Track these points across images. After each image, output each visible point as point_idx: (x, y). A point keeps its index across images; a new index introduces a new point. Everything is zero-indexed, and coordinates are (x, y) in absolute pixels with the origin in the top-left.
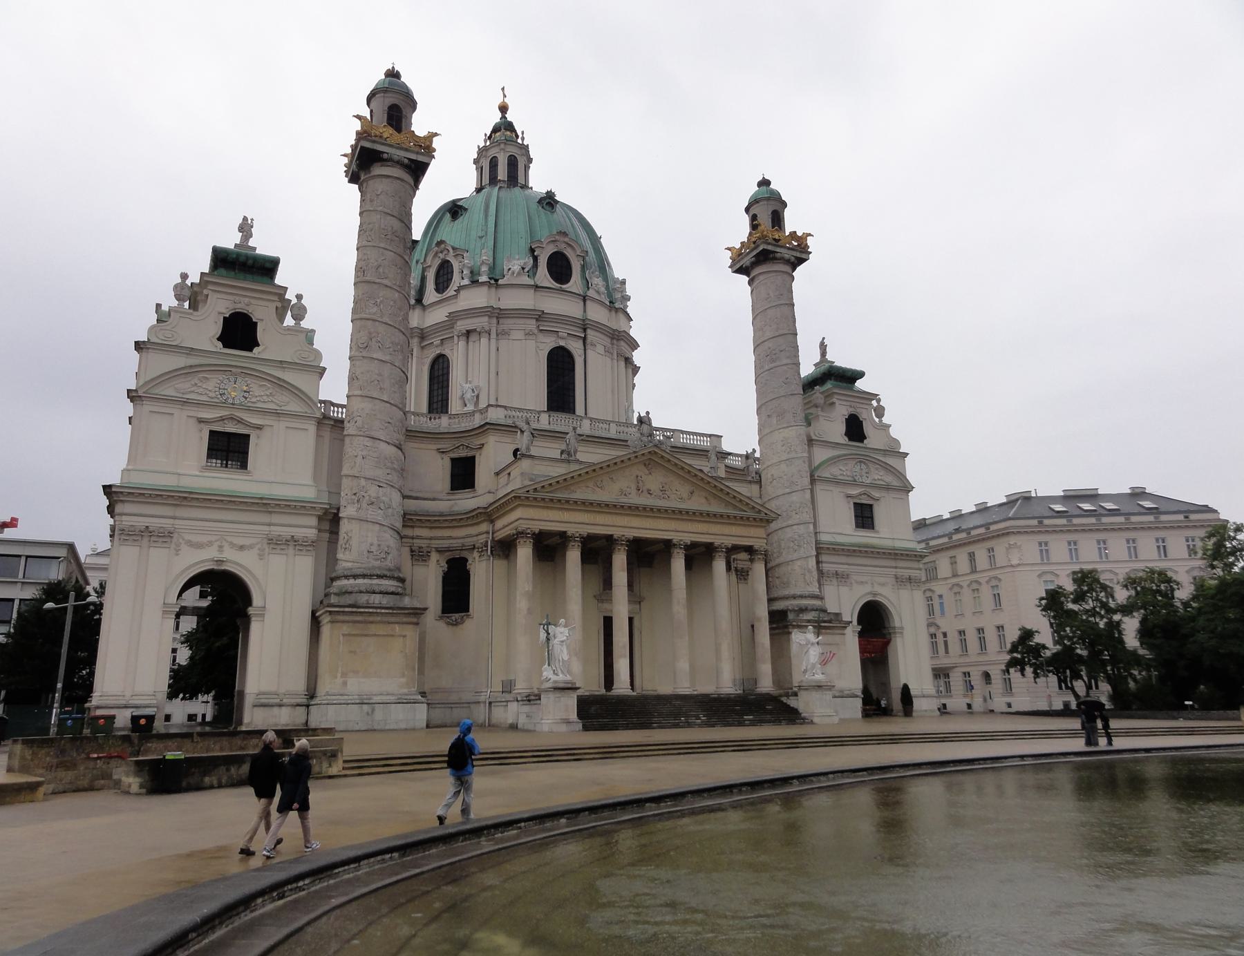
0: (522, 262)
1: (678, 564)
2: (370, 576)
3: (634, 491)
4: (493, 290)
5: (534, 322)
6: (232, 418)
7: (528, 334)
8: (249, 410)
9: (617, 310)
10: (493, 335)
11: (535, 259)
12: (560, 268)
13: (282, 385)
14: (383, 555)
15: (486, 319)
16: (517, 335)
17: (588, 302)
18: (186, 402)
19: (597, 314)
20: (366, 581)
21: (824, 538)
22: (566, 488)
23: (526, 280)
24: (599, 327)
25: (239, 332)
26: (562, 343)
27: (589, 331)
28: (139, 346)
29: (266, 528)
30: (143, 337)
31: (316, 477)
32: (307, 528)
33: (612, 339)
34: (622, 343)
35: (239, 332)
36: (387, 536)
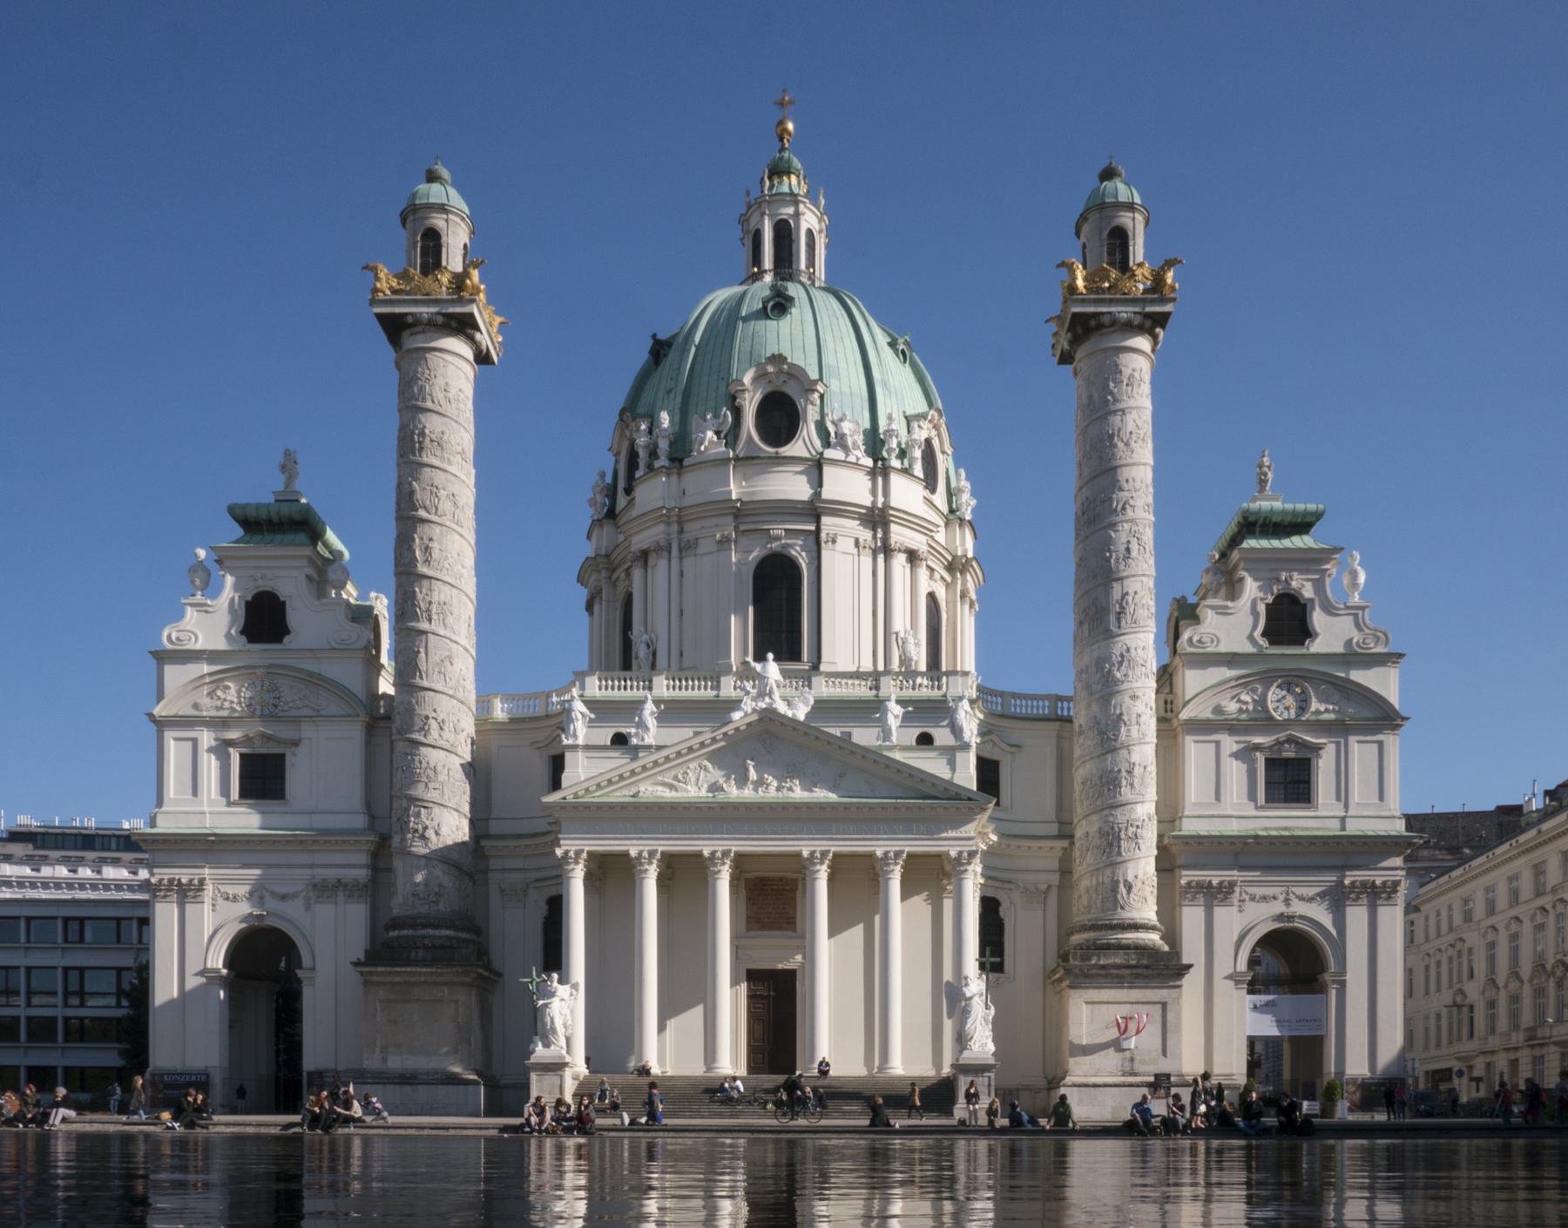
2: (414, 927)
4: (674, 478)
5: (731, 519)
11: (737, 412)
14: (432, 898)
15: (661, 528)
16: (705, 546)
17: (827, 470)
19: (848, 484)
20: (411, 932)
24: (840, 509)
27: (825, 520)
29: (306, 873)
31: (368, 805)
32: (353, 865)
36: (438, 872)
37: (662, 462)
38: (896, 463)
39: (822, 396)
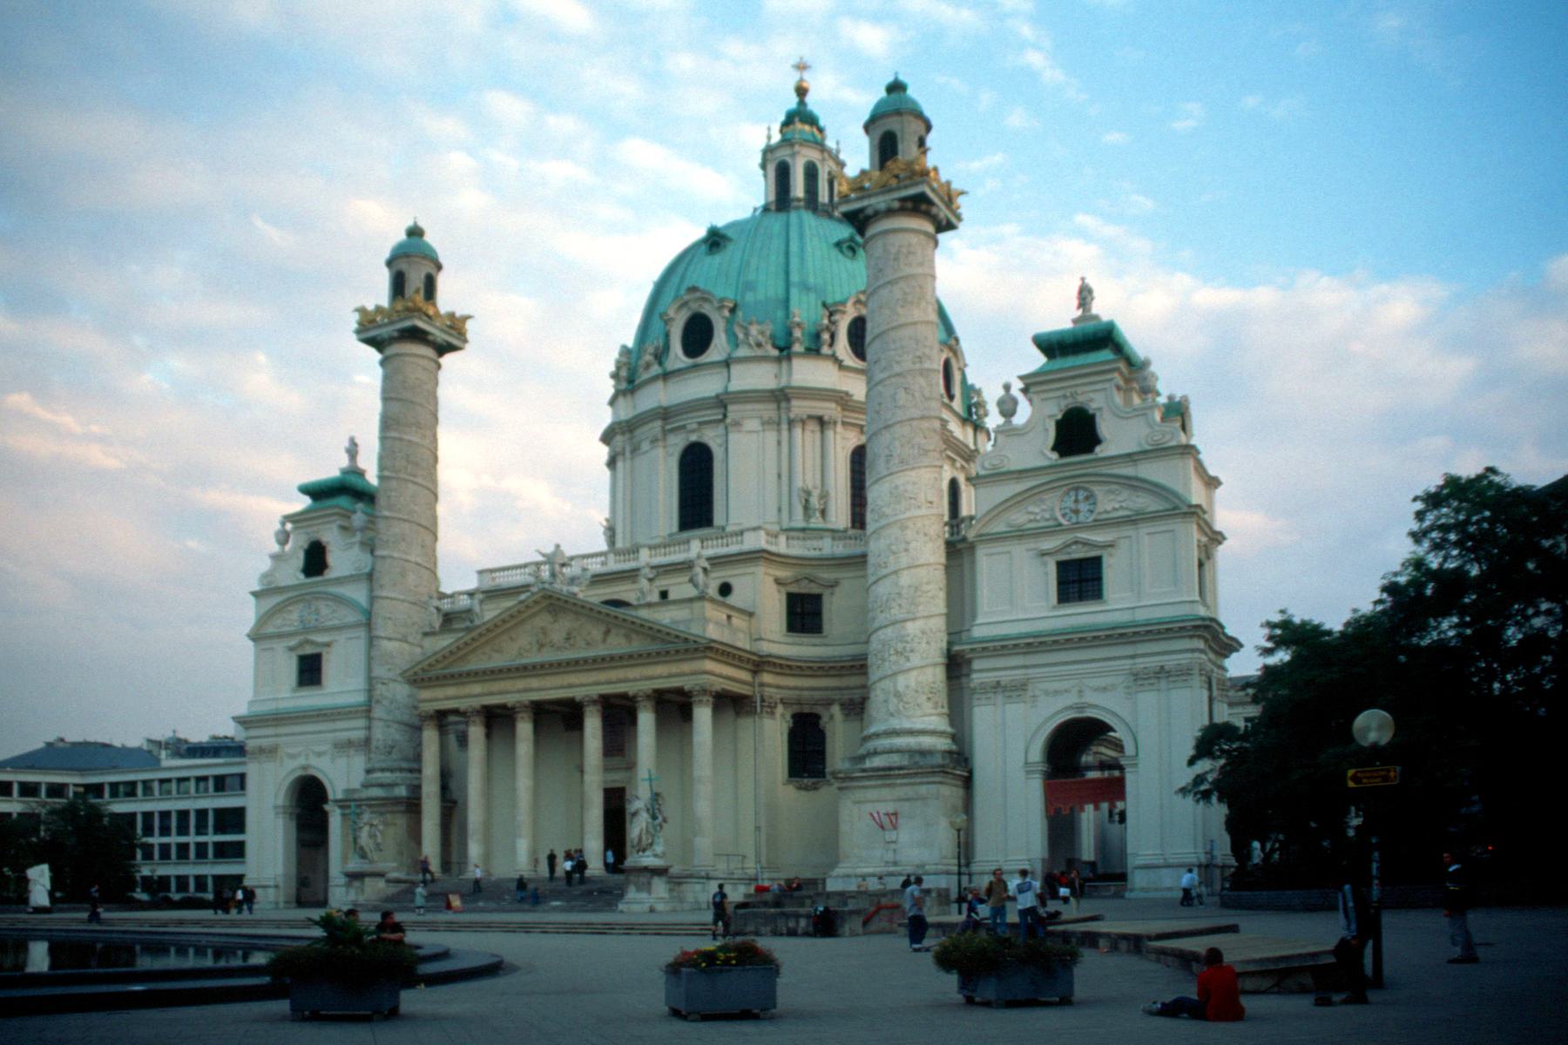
0: (651, 350)
1: (593, 725)
3: (535, 648)
4: (629, 397)
5: (658, 424)
6: (307, 642)
7: (654, 441)
8: (317, 630)
9: (789, 358)
10: (628, 454)
11: (667, 335)
12: (698, 335)
13: (339, 600)
16: (645, 446)
18: (280, 636)
21: (978, 632)
22: (462, 658)
23: (656, 370)
25: (315, 559)
26: (694, 438)
27: (731, 408)
28: (254, 594)
30: (257, 588)
33: (778, 402)
34: (794, 403)
35: (315, 559)
37: (624, 385)
38: (798, 348)
39: (733, 310)
